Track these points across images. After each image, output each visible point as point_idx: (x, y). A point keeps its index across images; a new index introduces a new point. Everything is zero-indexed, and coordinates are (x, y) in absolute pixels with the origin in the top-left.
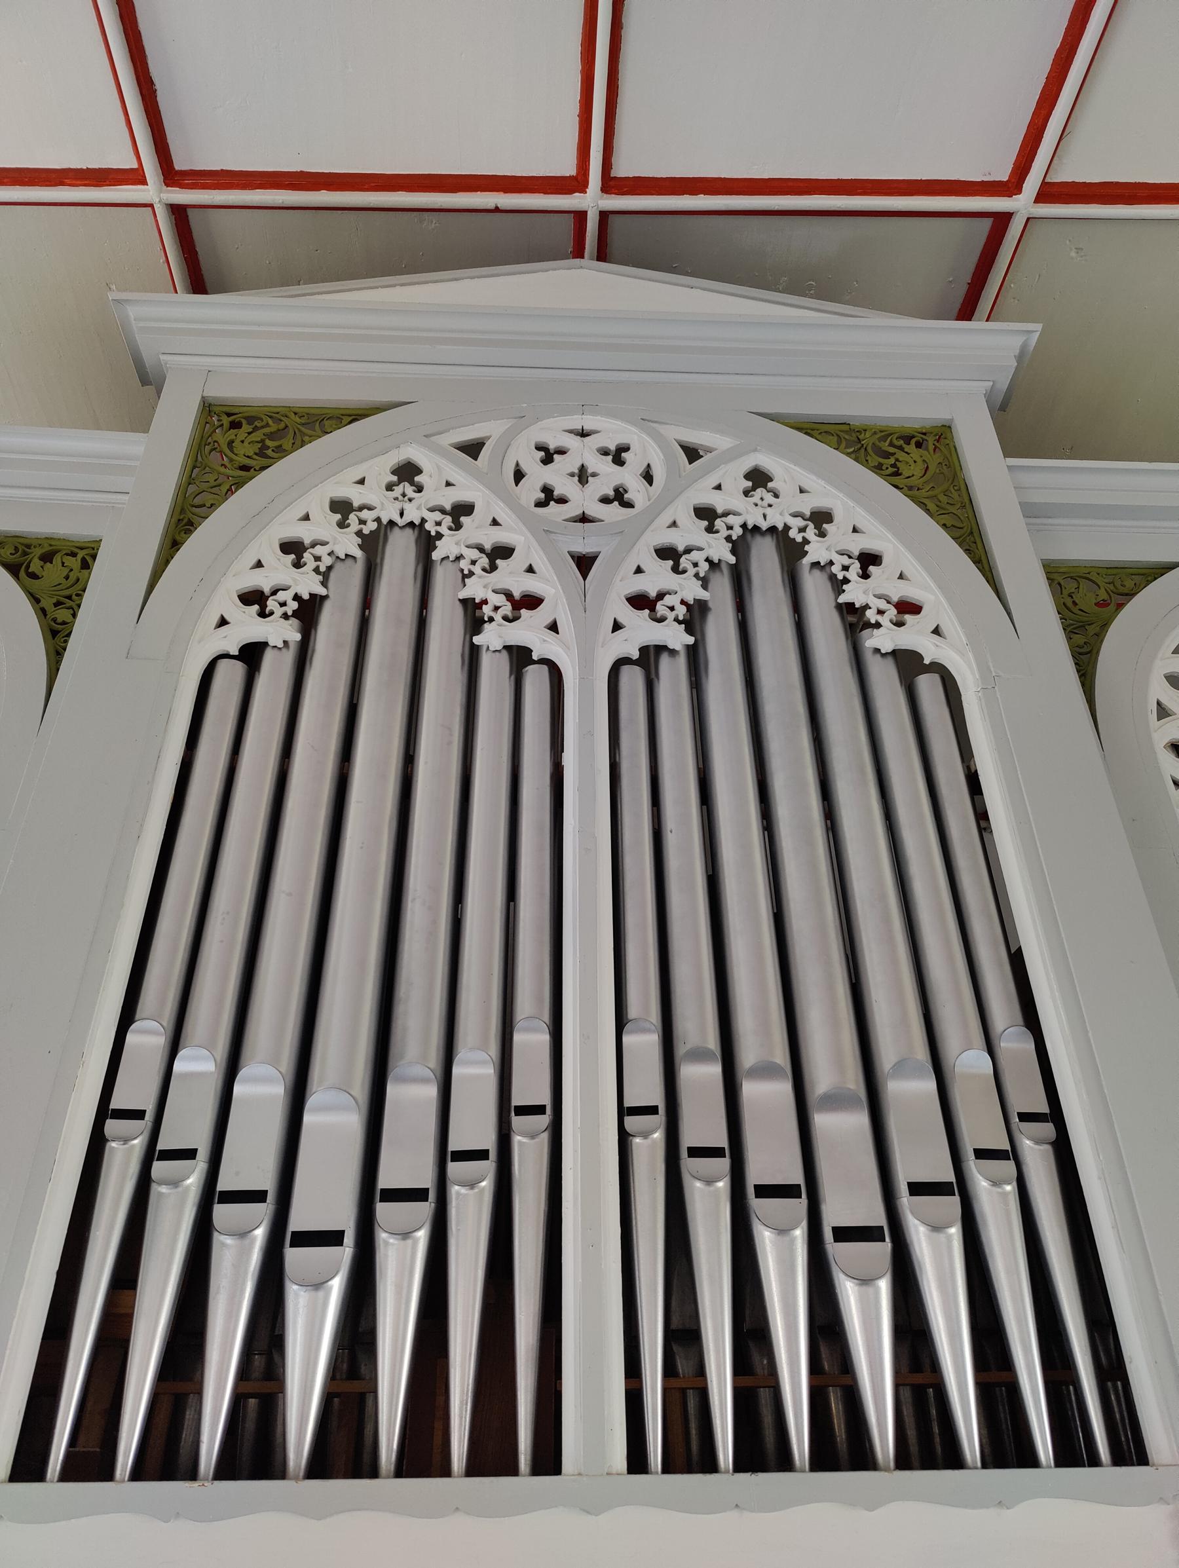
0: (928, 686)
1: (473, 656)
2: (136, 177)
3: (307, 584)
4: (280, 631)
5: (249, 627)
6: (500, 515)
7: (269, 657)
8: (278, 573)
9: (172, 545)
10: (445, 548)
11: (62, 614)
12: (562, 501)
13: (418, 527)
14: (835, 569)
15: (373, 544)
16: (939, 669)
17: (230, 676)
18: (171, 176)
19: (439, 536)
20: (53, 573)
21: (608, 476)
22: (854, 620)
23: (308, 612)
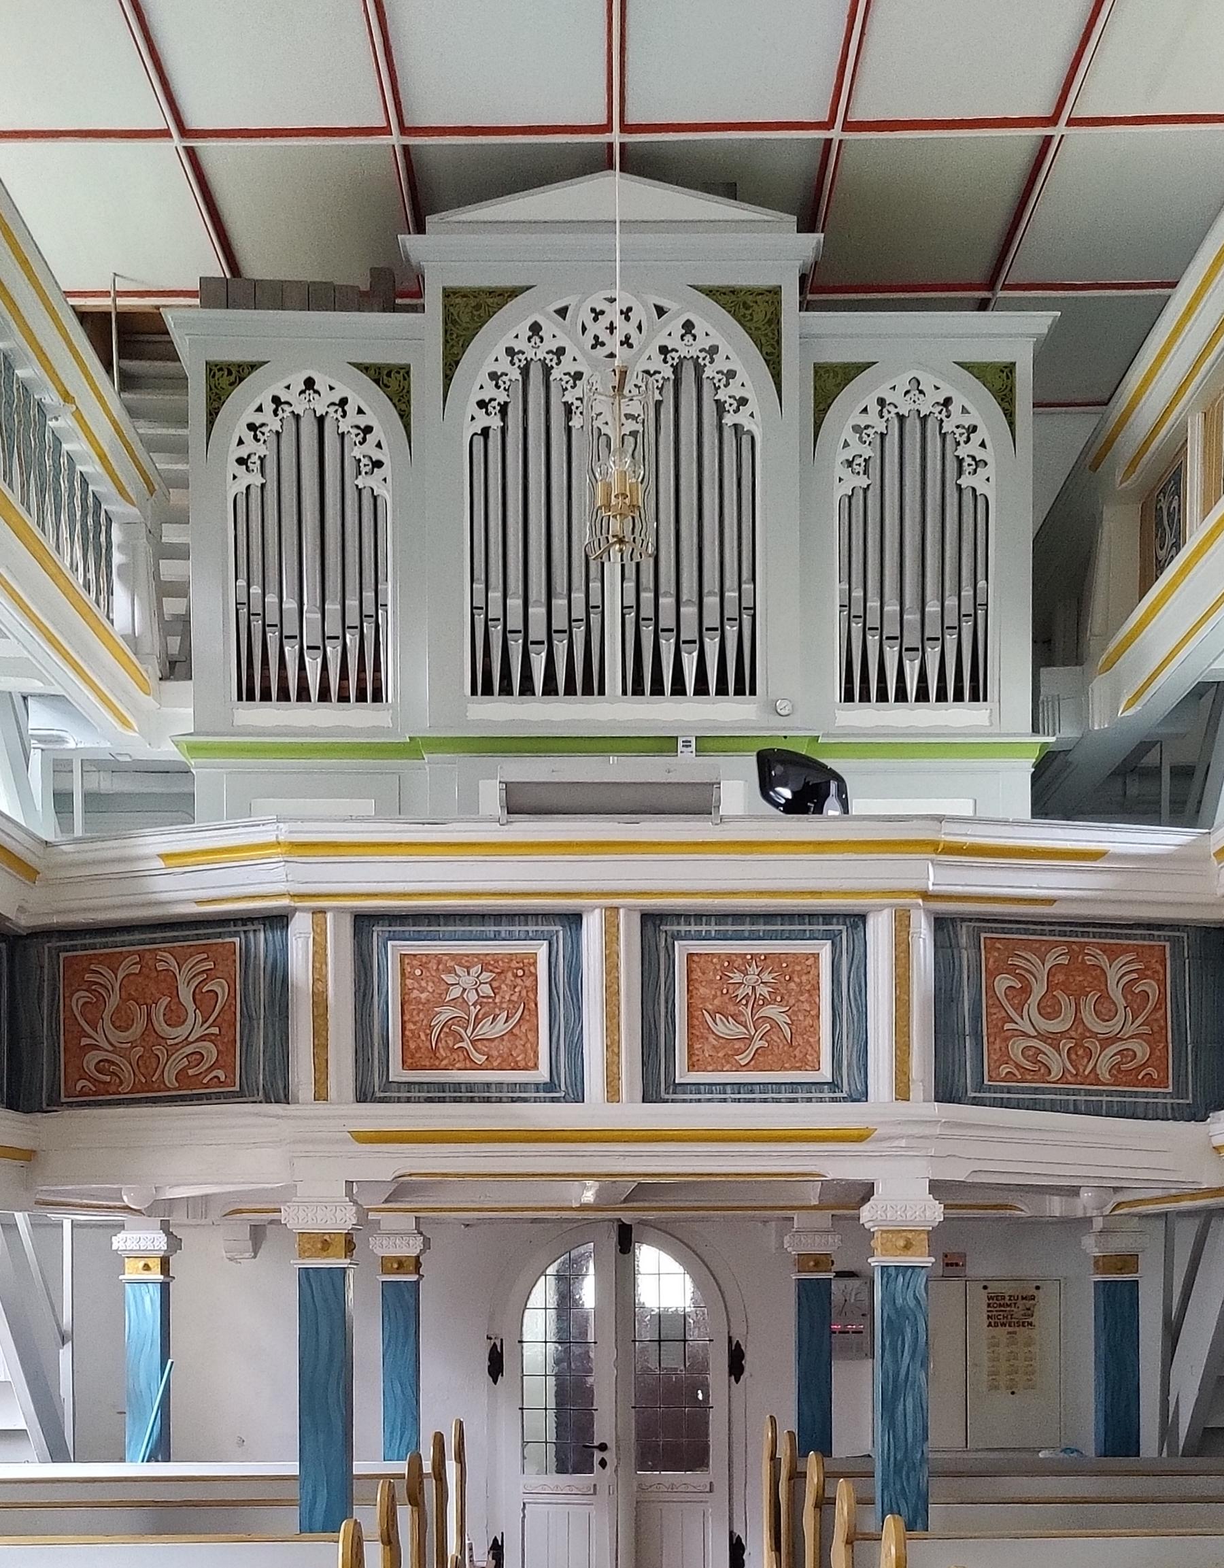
0: (746, 440)
1: (569, 430)
2: (386, 131)
3: (502, 397)
4: (495, 422)
5: (483, 420)
6: (578, 357)
7: (491, 432)
8: (489, 392)
9: (448, 378)
10: (556, 374)
11: (403, 407)
12: (603, 344)
13: (543, 362)
14: (716, 381)
15: (525, 371)
16: (749, 432)
17: (479, 441)
18: (404, 130)
19: (552, 367)
20: (393, 383)
21: (622, 328)
22: (720, 407)
23: (504, 409)
